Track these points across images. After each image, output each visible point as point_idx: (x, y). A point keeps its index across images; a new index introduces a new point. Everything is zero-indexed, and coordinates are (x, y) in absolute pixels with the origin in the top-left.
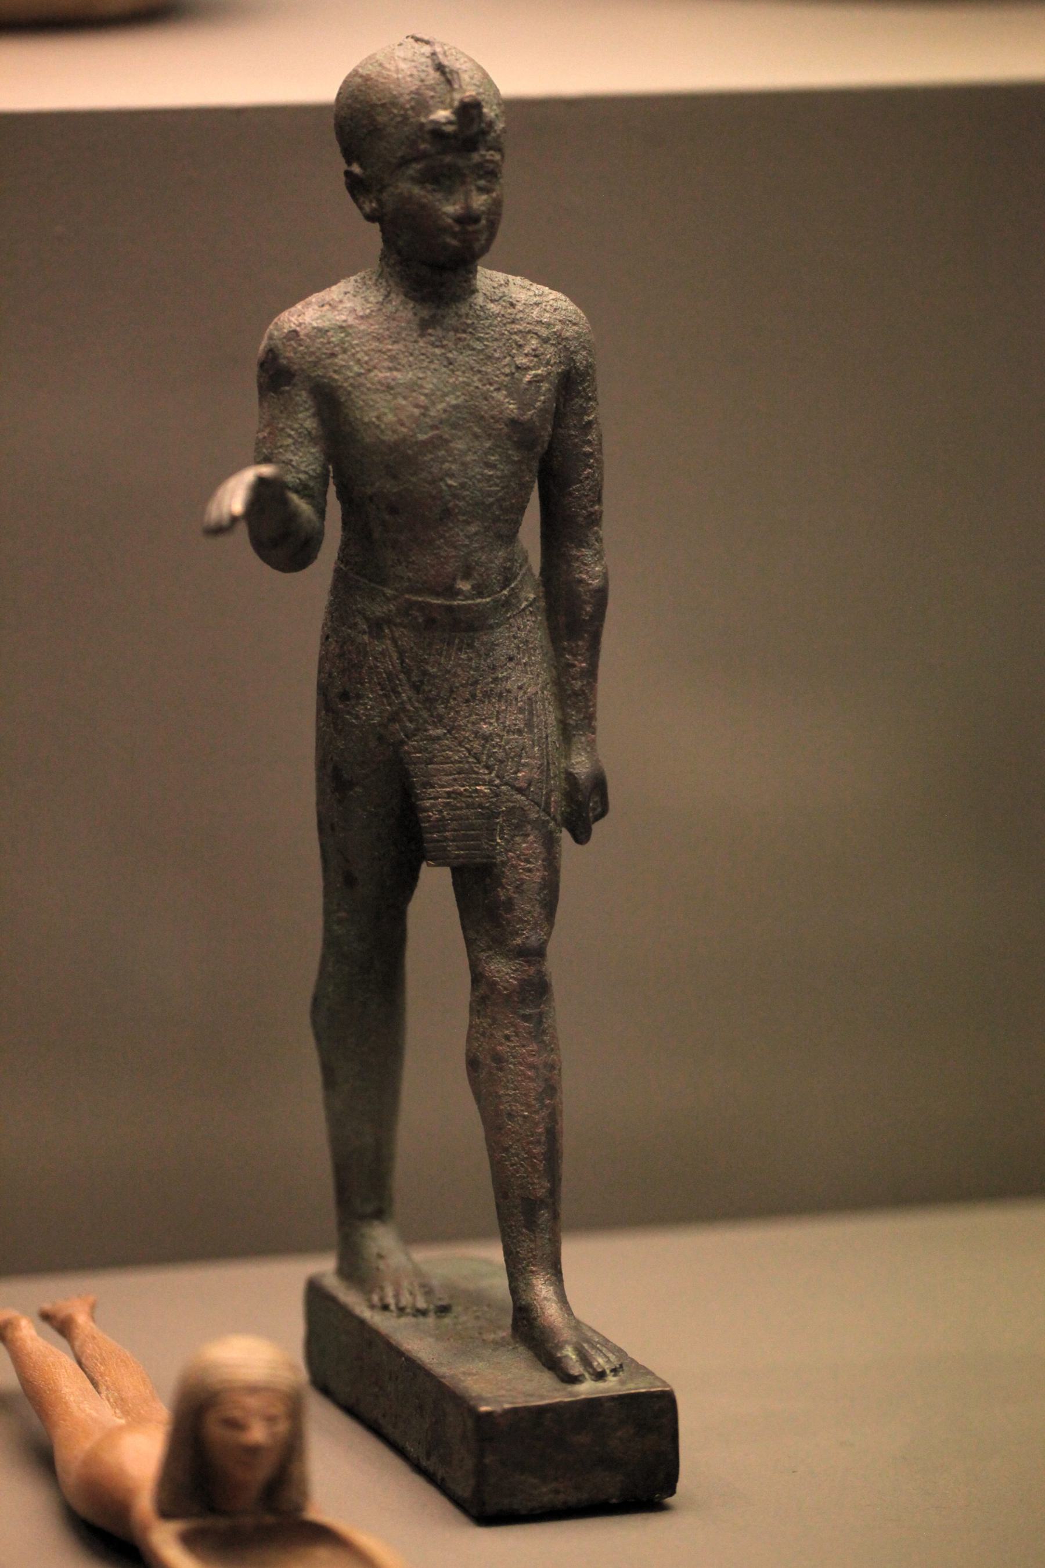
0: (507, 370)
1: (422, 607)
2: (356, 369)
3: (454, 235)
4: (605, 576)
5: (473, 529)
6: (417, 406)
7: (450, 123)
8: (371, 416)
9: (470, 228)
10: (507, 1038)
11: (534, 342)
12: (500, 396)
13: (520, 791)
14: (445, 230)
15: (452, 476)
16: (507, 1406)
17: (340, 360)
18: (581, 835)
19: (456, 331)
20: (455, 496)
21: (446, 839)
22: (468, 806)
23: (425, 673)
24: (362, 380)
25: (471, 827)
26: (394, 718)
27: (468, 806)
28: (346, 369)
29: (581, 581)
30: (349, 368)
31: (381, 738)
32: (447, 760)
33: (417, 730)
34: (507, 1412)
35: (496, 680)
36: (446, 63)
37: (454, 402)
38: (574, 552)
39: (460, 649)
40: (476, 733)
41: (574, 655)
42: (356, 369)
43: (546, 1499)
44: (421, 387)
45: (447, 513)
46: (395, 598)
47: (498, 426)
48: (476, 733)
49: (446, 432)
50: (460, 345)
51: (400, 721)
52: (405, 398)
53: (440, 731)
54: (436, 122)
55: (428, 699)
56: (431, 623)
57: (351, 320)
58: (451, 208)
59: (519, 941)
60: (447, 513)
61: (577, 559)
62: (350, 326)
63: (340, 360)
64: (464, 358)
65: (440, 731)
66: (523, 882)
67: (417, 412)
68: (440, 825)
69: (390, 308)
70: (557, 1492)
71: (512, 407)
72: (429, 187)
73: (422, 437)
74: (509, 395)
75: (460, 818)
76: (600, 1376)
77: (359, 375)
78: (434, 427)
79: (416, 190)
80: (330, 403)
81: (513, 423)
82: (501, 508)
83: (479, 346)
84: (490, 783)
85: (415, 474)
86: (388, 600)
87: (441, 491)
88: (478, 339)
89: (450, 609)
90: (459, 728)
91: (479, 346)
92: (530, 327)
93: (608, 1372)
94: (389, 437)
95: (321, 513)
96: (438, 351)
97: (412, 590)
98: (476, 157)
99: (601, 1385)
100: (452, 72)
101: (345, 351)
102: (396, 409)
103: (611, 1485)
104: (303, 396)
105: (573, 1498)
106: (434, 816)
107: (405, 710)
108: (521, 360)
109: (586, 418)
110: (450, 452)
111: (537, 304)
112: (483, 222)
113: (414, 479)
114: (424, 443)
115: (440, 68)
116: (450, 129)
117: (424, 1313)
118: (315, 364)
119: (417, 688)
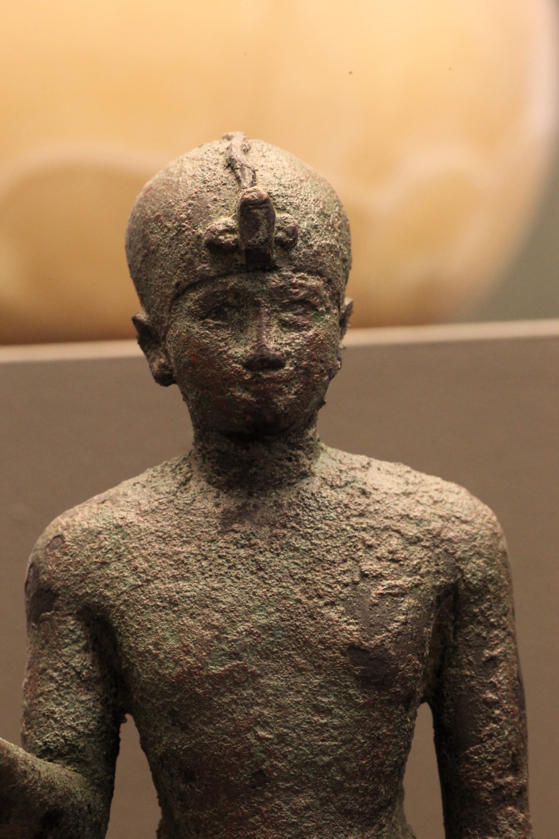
0: (347, 579)
3: (245, 385)
5: (302, 801)
6: (209, 627)
7: (229, 230)
8: (146, 643)
11: (395, 542)
12: (333, 614)
15: (265, 725)
20: (270, 753)
30: (122, 579)
37: (264, 621)
44: (216, 601)
47: (329, 654)
52: (192, 616)
57: (132, 517)
58: (240, 350)
60: (261, 778)
64: (284, 562)
67: (208, 634)
69: (185, 498)
71: (351, 630)
72: (211, 322)
73: (216, 669)
74: (349, 611)
78: (235, 655)
79: (196, 328)
80: (102, 628)
81: (353, 649)
82: (342, 770)
83: (302, 544)
91: (302, 544)
92: (387, 522)
94: (171, 671)
95: (106, 788)
98: (274, 280)
101: (119, 557)
108: (370, 565)
109: (487, 653)
110: (260, 690)
111: (407, 494)
113: (209, 730)
114: (221, 678)
115: (231, 165)
116: (230, 238)
118: (83, 578)
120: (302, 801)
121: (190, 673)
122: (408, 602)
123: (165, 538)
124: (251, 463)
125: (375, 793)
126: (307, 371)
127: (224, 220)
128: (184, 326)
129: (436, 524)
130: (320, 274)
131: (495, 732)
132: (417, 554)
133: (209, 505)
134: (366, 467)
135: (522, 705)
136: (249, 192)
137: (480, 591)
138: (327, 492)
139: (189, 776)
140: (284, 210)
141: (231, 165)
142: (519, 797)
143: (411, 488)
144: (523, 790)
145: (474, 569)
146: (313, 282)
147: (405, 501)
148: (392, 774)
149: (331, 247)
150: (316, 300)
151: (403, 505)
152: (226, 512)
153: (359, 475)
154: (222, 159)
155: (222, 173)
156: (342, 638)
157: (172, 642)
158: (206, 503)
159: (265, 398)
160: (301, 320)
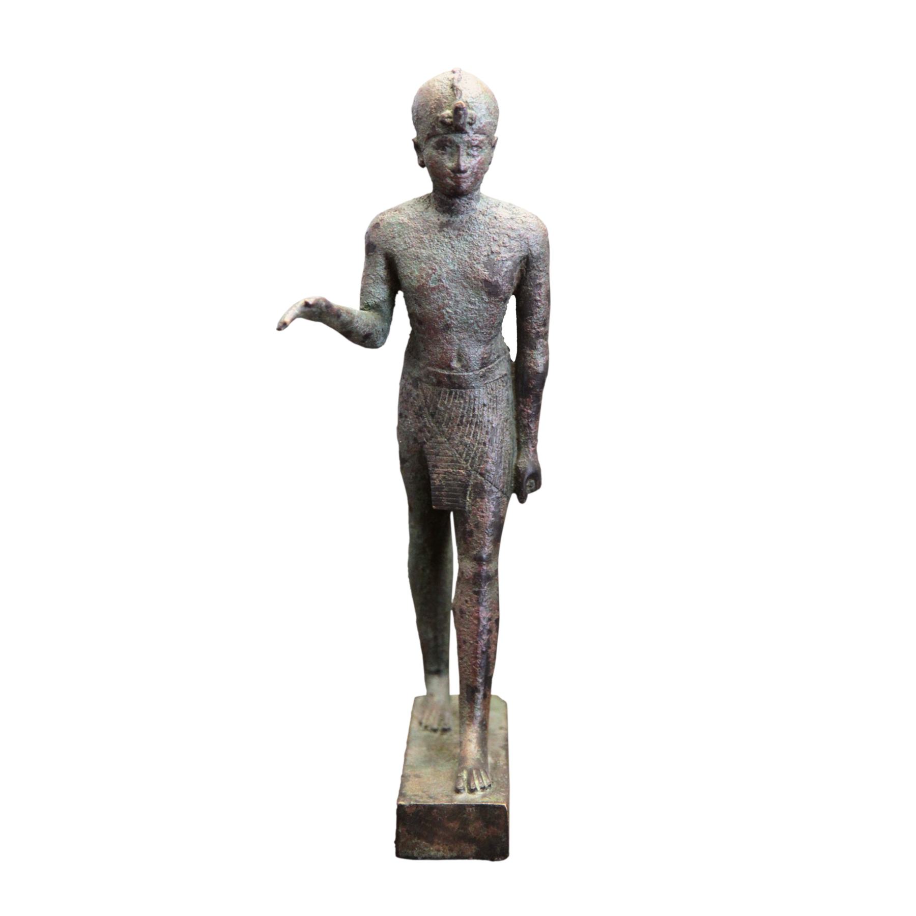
0: (485, 253)
1: (436, 374)
2: (403, 246)
3: (452, 178)
5: (461, 336)
7: (450, 117)
8: (407, 272)
9: (459, 175)
10: (466, 601)
11: (506, 239)
12: (478, 267)
13: (481, 475)
14: (445, 176)
15: (450, 307)
16: (412, 803)
17: (397, 240)
18: (522, 499)
19: (459, 230)
21: (442, 495)
22: (454, 480)
23: (437, 408)
24: (405, 253)
25: (455, 491)
26: (421, 430)
27: (454, 480)
28: (399, 246)
29: (530, 367)
31: (415, 440)
32: (446, 455)
33: (432, 437)
34: (411, 806)
35: (474, 416)
36: (456, 84)
37: (452, 268)
38: (528, 352)
39: (455, 398)
40: (461, 442)
41: (525, 406)
42: (403, 246)
44: (434, 259)
45: (448, 327)
46: (424, 368)
47: (476, 282)
48: (461, 442)
49: (446, 283)
50: (460, 238)
51: (424, 432)
53: (444, 439)
54: (443, 117)
55: (437, 422)
56: (439, 383)
57: (406, 220)
58: (450, 164)
59: (475, 552)
60: (448, 327)
61: (529, 355)
62: (404, 223)
63: (397, 240)
64: (462, 245)
65: (444, 439)
66: (479, 522)
68: (440, 489)
70: (439, 851)
71: (486, 274)
72: (440, 152)
74: (486, 267)
75: (449, 485)
76: (472, 791)
77: (404, 249)
79: (434, 153)
81: (486, 281)
83: (469, 239)
84: (466, 469)
85: (430, 304)
86: (421, 369)
88: (471, 235)
89: (449, 376)
90: (453, 439)
91: (469, 239)
94: (415, 284)
95: (389, 320)
96: (446, 240)
97: (430, 365)
98: (465, 137)
99: (471, 796)
100: (457, 89)
101: (400, 236)
102: (422, 269)
104: (381, 260)
106: (437, 482)
107: (425, 426)
108: (495, 248)
109: (538, 281)
111: (512, 219)
112: (469, 173)
114: (434, 289)
115: (453, 87)
116: (448, 120)
117: (435, 731)
119: (433, 415)
121: (423, 286)
122: (509, 263)
123: (417, 231)
124: (453, 205)
125: (490, 333)
126: (476, 173)
127: (448, 112)
128: (429, 151)
129: (522, 232)
131: (537, 318)
132: (514, 244)
133: (435, 219)
135: (549, 301)
136: (460, 101)
137: (538, 258)
138: (481, 217)
139: (420, 323)
140: (472, 109)
141: (453, 87)
143: (514, 216)
144: (546, 333)
145: (536, 250)
146: (482, 137)
148: (497, 327)
149: (489, 123)
150: (481, 145)
151: (510, 223)
152: (442, 223)
153: (494, 210)
154: (449, 83)
155: (449, 90)
156: (481, 277)
157: (417, 273)
158: (434, 217)
159: (458, 185)
160: (476, 153)
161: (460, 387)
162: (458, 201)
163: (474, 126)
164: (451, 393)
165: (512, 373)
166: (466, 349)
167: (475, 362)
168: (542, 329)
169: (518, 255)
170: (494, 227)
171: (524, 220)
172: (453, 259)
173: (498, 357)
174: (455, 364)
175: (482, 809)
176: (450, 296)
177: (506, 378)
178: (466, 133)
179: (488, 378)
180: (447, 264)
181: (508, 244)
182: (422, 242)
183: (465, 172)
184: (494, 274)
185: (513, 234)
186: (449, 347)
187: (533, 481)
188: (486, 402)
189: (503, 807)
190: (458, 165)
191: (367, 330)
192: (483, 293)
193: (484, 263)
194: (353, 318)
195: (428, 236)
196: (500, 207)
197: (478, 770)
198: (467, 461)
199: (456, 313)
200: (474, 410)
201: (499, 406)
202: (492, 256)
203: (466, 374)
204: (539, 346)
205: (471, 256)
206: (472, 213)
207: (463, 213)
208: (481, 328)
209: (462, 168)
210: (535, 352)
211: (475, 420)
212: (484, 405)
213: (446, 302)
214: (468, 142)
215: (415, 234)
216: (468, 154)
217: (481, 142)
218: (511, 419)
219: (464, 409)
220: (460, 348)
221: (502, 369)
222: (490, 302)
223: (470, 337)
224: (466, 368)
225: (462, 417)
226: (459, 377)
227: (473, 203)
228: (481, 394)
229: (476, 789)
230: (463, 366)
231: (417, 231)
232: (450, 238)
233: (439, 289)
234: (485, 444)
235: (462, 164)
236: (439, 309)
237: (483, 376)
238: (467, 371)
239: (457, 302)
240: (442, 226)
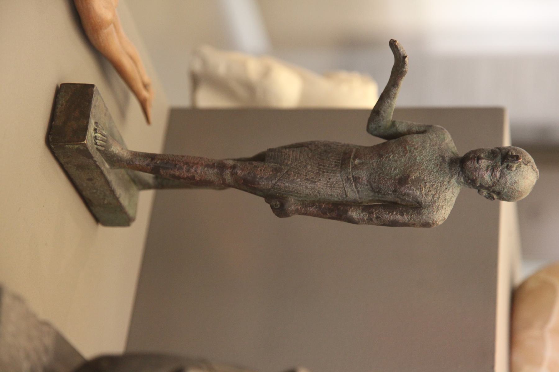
0: (425, 178)
3: (474, 156)
4: (351, 221)
5: (375, 164)
6: (418, 147)
11: (433, 193)
12: (417, 173)
13: (287, 172)
15: (393, 157)
20: (387, 157)
23: (329, 153)
28: (432, 136)
35: (324, 172)
39: (336, 162)
40: (308, 164)
43: (60, 102)
47: (408, 171)
49: (408, 155)
64: (431, 166)
67: (416, 147)
70: (62, 105)
73: (407, 147)
74: (417, 177)
78: (410, 152)
82: (381, 173)
83: (435, 170)
84: (291, 164)
87: (389, 153)
88: (437, 171)
89: (350, 157)
93: (96, 135)
99: (92, 128)
103: (58, 122)
105: (58, 111)
110: (402, 156)
111: (445, 200)
112: (477, 165)
113: (394, 146)
114: (405, 148)
120: (375, 164)
125: (374, 182)
129: (437, 204)
130: (500, 178)
134: (453, 192)
142: (370, 221)
147: (444, 198)
153: (451, 190)
161: (342, 164)
162: (458, 165)
163: (505, 170)
164: (338, 160)
165: (347, 202)
166: (366, 167)
167: (356, 173)
168: (375, 216)
169: (423, 199)
170: (441, 186)
171: (444, 207)
172: (423, 160)
173: (358, 192)
174: (357, 161)
175: (86, 129)
176: (400, 157)
177: (344, 196)
178: (502, 164)
179: (346, 182)
180: (420, 156)
181: (430, 193)
182: (433, 146)
183: (478, 162)
184: (413, 181)
185: (437, 196)
186: (368, 158)
187: (279, 206)
188: (331, 180)
189: (84, 140)
190: (483, 159)
191: (382, 112)
192: (401, 175)
193: (420, 177)
194: (391, 99)
195: (437, 149)
196: (451, 195)
197: (106, 141)
198: (296, 165)
199: (390, 160)
200: (327, 172)
201: (328, 188)
202: (423, 182)
203: (351, 167)
204: (364, 213)
205: (424, 170)
206: (449, 175)
207: (450, 169)
208: (379, 175)
209: (480, 161)
210: (360, 211)
211: (321, 172)
212: (330, 179)
213: (397, 155)
214: (496, 166)
215: (438, 143)
216: (488, 166)
217: (495, 176)
218: (319, 197)
219: (328, 167)
220: (367, 164)
221: (352, 194)
222: (395, 180)
223: (374, 169)
224: (355, 167)
225: (324, 166)
226: (349, 163)
227: (456, 177)
228: (337, 177)
229: (96, 133)
230: (355, 165)
231: (440, 145)
232: (436, 160)
233: (405, 151)
234: (306, 176)
235: (483, 161)
236: (392, 151)
237: (348, 179)
238: (353, 168)
239: (396, 161)
240: (443, 158)
